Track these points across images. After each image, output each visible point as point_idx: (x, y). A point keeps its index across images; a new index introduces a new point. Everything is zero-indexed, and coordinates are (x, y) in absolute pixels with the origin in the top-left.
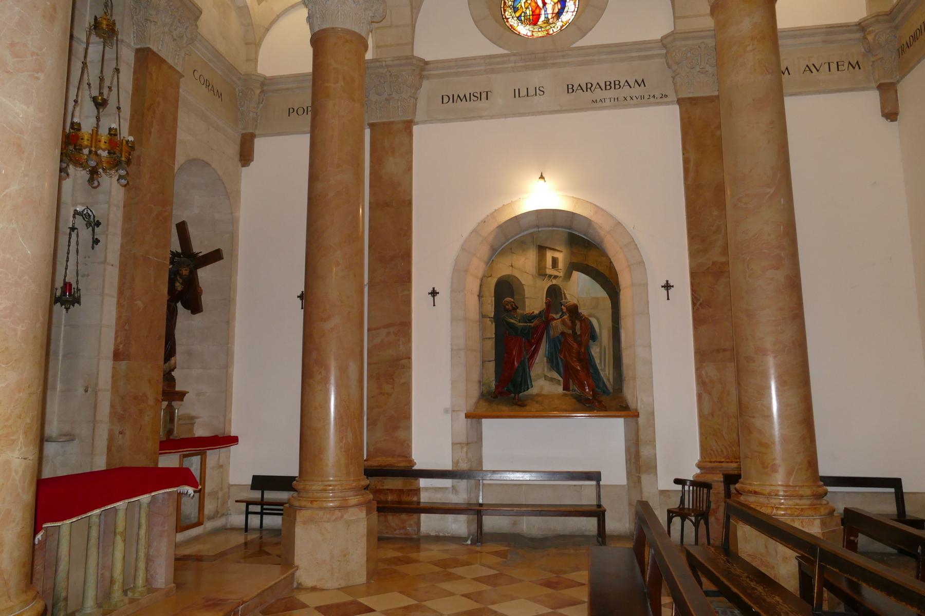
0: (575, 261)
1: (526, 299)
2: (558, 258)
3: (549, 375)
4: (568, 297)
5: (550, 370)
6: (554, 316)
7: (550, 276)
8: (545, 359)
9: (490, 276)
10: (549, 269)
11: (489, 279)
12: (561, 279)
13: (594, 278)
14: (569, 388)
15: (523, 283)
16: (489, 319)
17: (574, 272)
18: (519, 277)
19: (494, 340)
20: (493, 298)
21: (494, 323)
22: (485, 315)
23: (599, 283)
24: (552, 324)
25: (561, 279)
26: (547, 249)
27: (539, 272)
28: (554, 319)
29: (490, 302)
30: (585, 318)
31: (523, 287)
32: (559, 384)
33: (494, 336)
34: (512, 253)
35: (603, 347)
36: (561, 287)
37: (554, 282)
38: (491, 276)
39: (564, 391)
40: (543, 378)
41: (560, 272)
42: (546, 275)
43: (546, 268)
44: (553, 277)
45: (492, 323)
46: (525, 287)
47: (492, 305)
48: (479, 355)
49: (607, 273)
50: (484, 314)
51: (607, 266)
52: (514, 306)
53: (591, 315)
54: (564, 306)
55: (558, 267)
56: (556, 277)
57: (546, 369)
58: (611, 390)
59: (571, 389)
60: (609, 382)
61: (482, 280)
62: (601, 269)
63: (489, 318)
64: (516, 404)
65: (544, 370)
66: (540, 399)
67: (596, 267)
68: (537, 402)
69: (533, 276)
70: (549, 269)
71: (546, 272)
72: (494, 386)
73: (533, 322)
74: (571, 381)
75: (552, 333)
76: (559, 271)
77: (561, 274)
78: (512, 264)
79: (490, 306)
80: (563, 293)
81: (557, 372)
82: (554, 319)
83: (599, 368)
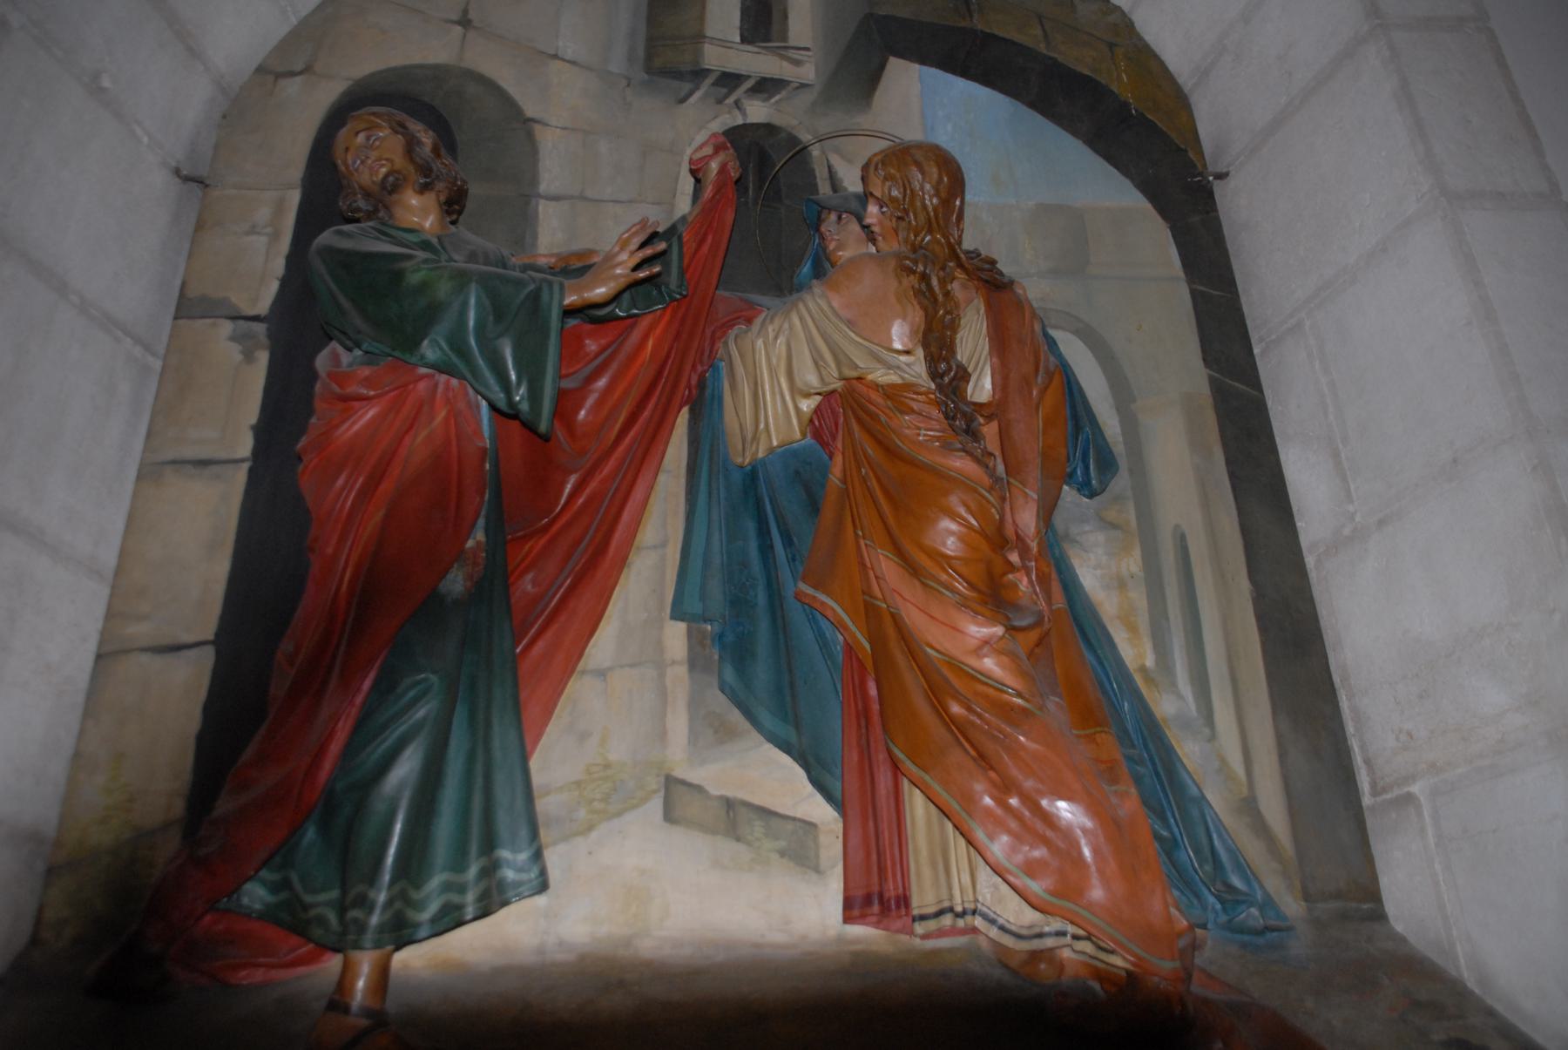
1: (543, 207)
5: (725, 734)
7: (730, 80)
8: (676, 636)
9: (301, 73)
10: (724, 43)
11: (292, 87)
12: (807, 97)
13: (1043, 105)
14: (904, 901)
15: (530, 111)
16: (227, 327)
17: (895, 64)
19: (241, 476)
20: (295, 197)
21: (263, 358)
23: (1075, 133)
25: (807, 97)
27: (649, 57)
29: (263, 214)
31: (530, 136)
33: (245, 446)
37: (758, 111)
38: (307, 70)
39: (857, 930)
40: (656, 805)
41: (797, 63)
42: (699, 74)
43: (700, 37)
44: (749, 84)
45: (249, 357)
47: (275, 237)
49: (1121, 83)
51: (1111, 46)
55: (784, 38)
56: (766, 87)
57: (678, 723)
58: (1292, 907)
59: (924, 898)
60: (1261, 828)
62: (1079, 59)
65: (662, 735)
70: (724, 43)
74: (917, 806)
75: (736, 413)
76: (793, 54)
78: (465, 12)
79: (260, 241)
81: (786, 748)
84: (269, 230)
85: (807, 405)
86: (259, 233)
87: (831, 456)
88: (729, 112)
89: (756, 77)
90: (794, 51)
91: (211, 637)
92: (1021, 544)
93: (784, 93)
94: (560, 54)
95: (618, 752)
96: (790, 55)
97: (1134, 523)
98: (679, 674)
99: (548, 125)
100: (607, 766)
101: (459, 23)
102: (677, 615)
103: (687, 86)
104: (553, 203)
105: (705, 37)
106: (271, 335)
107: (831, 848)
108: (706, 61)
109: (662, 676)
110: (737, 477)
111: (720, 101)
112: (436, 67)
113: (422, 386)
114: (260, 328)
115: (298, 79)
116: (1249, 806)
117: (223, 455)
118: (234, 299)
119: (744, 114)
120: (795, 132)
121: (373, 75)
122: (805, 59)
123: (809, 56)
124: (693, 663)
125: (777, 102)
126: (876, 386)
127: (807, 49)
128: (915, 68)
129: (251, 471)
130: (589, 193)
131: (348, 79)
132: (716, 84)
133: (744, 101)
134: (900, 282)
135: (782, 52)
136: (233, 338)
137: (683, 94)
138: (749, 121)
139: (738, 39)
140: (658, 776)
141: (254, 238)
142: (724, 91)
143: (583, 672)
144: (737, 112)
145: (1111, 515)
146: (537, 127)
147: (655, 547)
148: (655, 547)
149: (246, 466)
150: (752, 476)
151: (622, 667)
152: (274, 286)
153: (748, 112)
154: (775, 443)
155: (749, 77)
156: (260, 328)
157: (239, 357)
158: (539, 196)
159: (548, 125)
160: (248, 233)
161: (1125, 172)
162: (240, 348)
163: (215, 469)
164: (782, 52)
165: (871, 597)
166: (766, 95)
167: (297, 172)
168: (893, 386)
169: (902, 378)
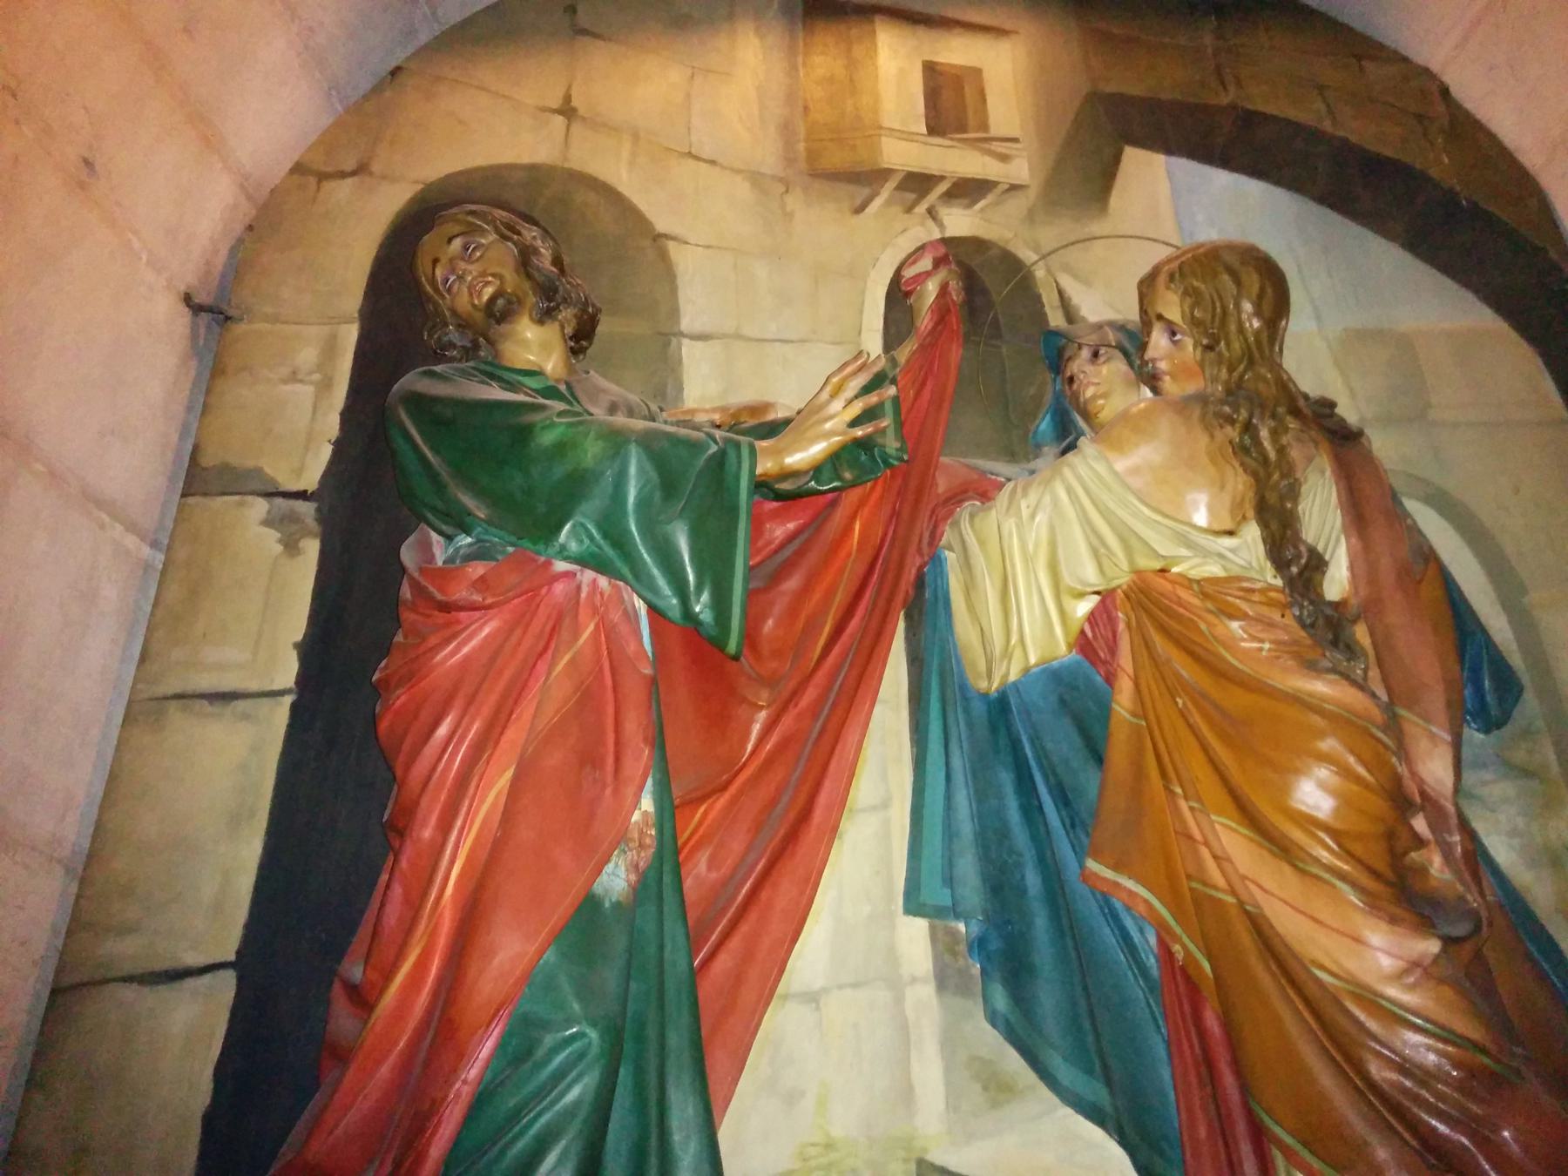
1: (691, 353)
7: (918, 183)
9: (354, 173)
11: (342, 190)
15: (661, 225)
16: (260, 506)
17: (1134, 158)
19: (279, 715)
21: (312, 549)
22: (225, 469)
25: (1017, 206)
26: (878, 19)
29: (307, 356)
31: (664, 256)
33: (287, 672)
34: (584, 32)
37: (960, 222)
38: (361, 170)
41: (1004, 158)
44: (943, 187)
45: (291, 546)
47: (326, 385)
50: (208, 459)
55: (984, 126)
56: (968, 190)
57: (929, 1074)
63: (273, 494)
69: (756, 178)
70: (908, 136)
76: (998, 147)
77: (1020, 169)
84: (316, 377)
85: (1084, 607)
86: (301, 381)
87: (1110, 679)
88: (923, 224)
89: (953, 177)
90: (998, 143)
91: (232, 957)
92: (1429, 803)
93: (990, 198)
94: (693, 151)
95: (843, 1123)
96: (993, 148)
97: (1555, 768)
98: (923, 995)
99: (687, 243)
100: (829, 1146)
101: (559, 112)
102: (914, 905)
103: (865, 192)
104: (700, 344)
105: (881, 128)
106: (323, 518)
108: (886, 159)
109: (899, 1000)
110: (979, 708)
111: (909, 210)
112: (533, 168)
113: (559, 588)
114: (307, 509)
115: (349, 181)
117: (254, 686)
118: (268, 470)
119: (941, 226)
120: (1012, 248)
121: (448, 177)
122: (1014, 152)
123: (1017, 149)
124: (944, 979)
125: (982, 210)
126: (1187, 582)
127: (1015, 140)
128: (1159, 159)
129: (295, 707)
130: (748, 331)
131: (416, 182)
132: (901, 187)
133: (938, 208)
134: (1212, 436)
135: (986, 146)
136: (267, 523)
137: (858, 202)
138: (948, 234)
139: (924, 131)
140: (906, 1161)
141: (298, 387)
142: (912, 196)
143: (786, 997)
144: (930, 223)
145: (1519, 756)
146: (672, 246)
147: (874, 808)
148: (874, 808)
149: (288, 700)
150: (1000, 706)
151: (840, 987)
152: (326, 452)
153: (945, 222)
154: (1033, 660)
155: (942, 178)
156: (307, 509)
157: (279, 548)
158: (682, 335)
159: (687, 243)
160: (285, 382)
161: (1466, 284)
162: (279, 535)
163: (241, 705)
164: (984, 142)
165: (1205, 884)
166: (966, 201)
167: (352, 299)
168: (1214, 581)
169: (1225, 569)
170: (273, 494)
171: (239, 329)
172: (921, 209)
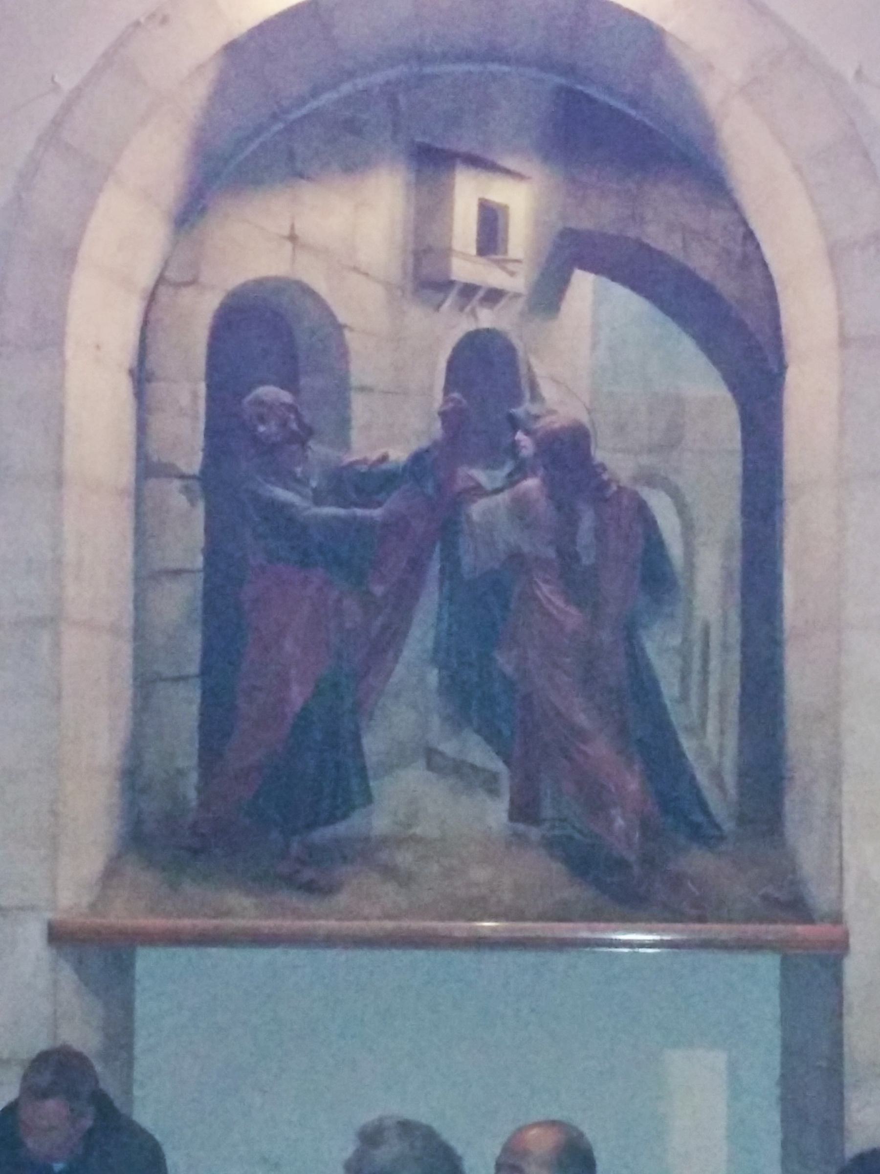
0: (585, 223)
2: (505, 209)
3: (449, 748)
4: (548, 391)
6: (481, 476)
7: (469, 291)
8: (433, 677)
10: (465, 256)
11: (187, 296)
12: (520, 305)
15: (342, 317)
16: (177, 484)
18: (321, 286)
20: (202, 388)
24: (468, 517)
28: (478, 491)
29: (185, 400)
30: (620, 489)
31: (341, 335)
32: (494, 793)
33: (199, 561)
34: (301, 176)
35: (698, 626)
36: (516, 341)
37: (486, 318)
38: (193, 282)
41: (512, 274)
43: (447, 252)
44: (481, 294)
45: (192, 502)
46: (348, 334)
47: (195, 418)
48: (126, 649)
52: (294, 426)
53: (651, 479)
54: (527, 433)
55: (506, 252)
56: (494, 296)
57: (435, 721)
58: (729, 826)
60: (721, 786)
61: (152, 298)
64: (291, 881)
66: (404, 858)
67: (680, 256)
68: (389, 872)
69: (388, 285)
70: (465, 256)
71: (448, 269)
72: (192, 794)
73: (380, 504)
76: (511, 267)
78: (292, 227)
80: (523, 370)
82: (478, 491)
83: (677, 716)
102: (434, 661)
103: (441, 296)
107: (505, 784)
111: (462, 309)
112: (277, 279)
116: (716, 775)
136: (181, 492)
139: (473, 251)
156: (196, 486)
164: (502, 264)
170: (182, 477)
171: (154, 385)
172: (468, 309)
